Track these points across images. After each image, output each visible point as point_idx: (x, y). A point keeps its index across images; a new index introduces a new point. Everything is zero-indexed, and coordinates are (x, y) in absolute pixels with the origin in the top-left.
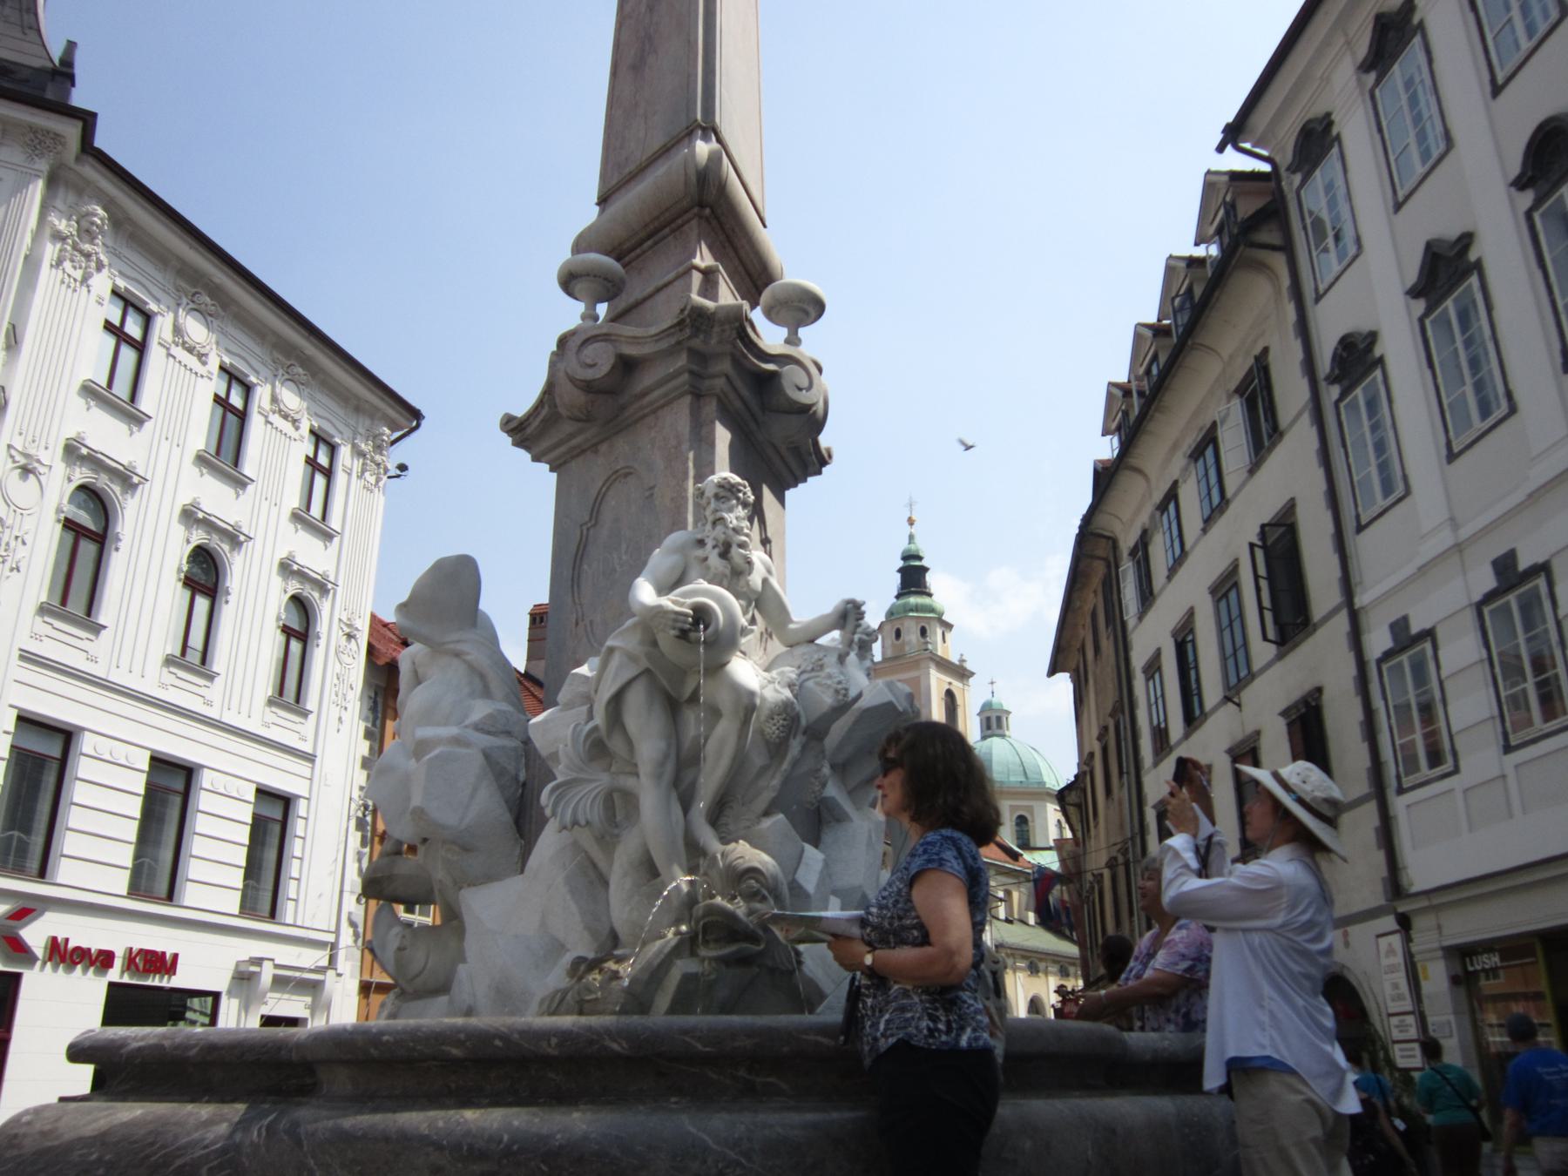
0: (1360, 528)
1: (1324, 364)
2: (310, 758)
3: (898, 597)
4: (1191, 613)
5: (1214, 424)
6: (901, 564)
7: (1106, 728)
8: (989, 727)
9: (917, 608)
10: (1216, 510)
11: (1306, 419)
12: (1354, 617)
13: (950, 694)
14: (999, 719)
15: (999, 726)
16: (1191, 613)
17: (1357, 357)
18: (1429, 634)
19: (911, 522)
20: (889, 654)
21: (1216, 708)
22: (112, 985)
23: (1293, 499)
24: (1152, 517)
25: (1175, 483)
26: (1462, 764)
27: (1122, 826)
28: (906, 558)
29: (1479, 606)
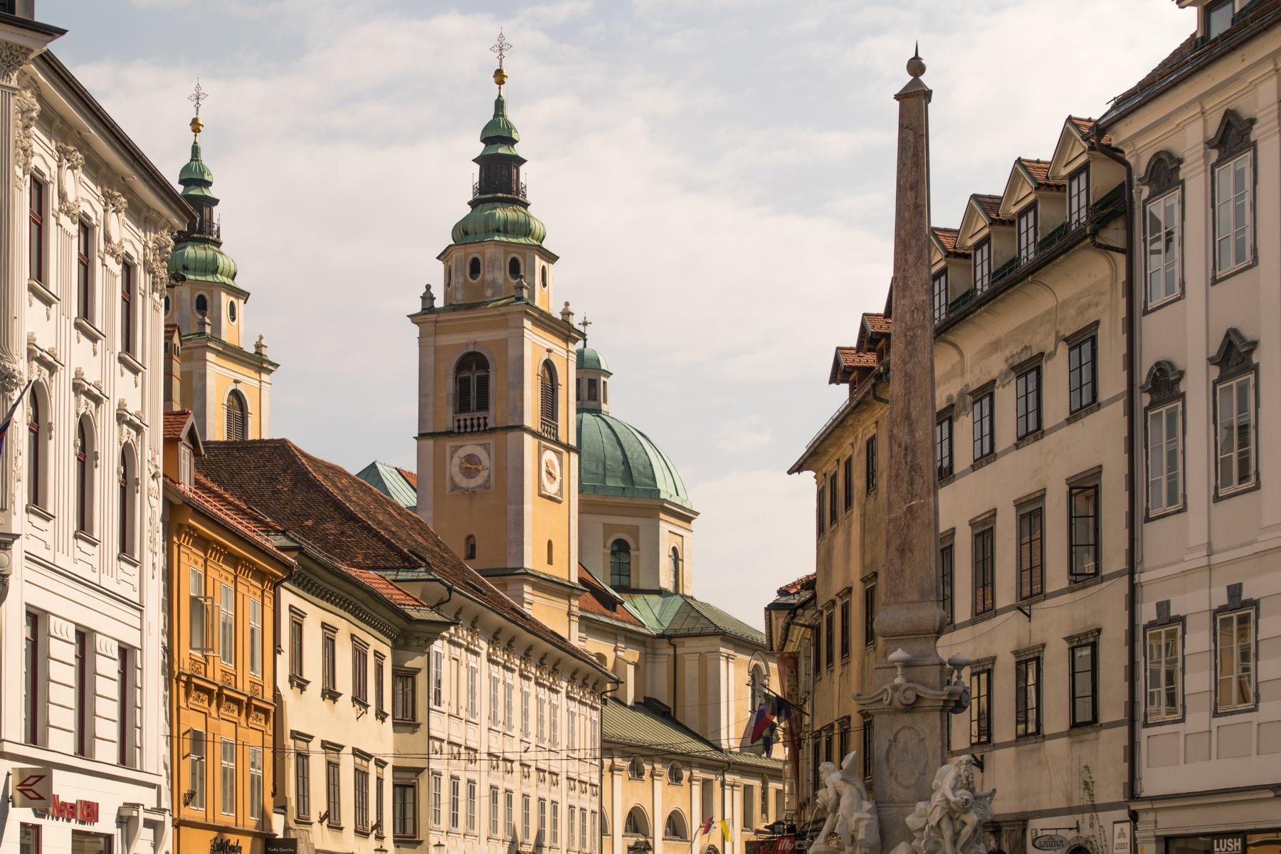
0: (1148, 519)
2: (139, 607)
3: (473, 204)
4: (993, 513)
6: (479, 148)
9: (507, 228)
11: (1119, 407)
12: (1133, 588)
13: (548, 365)
16: (993, 513)
18: (1182, 620)
20: (460, 297)
22: (75, 832)
23: (1100, 466)
24: (962, 395)
25: (994, 381)
26: (1187, 716)
29: (1216, 613)
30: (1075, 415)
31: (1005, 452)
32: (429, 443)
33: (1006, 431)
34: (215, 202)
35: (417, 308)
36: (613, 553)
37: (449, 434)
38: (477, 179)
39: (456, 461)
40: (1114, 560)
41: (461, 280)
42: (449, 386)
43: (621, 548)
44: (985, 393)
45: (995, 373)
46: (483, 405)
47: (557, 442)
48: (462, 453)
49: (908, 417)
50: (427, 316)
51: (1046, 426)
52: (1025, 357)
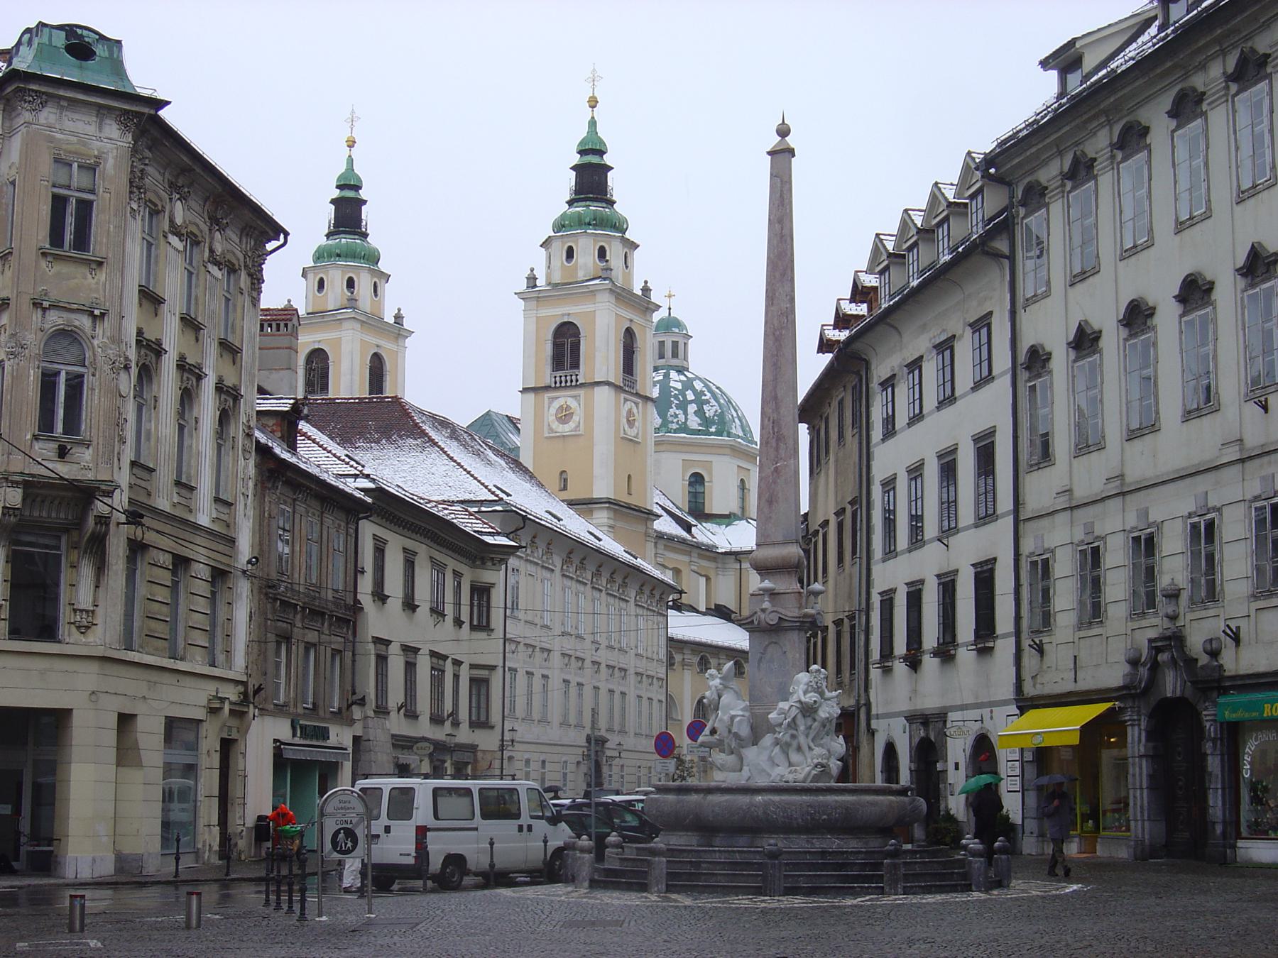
1: (1022, 357)
5: (954, 336)
7: (844, 510)
8: (662, 356)
10: (948, 399)
11: (1007, 379)
13: (629, 333)
14: (675, 344)
15: (675, 355)
17: (1037, 360)
19: (593, 103)
20: (557, 278)
21: (931, 541)
24: (900, 367)
27: (850, 597)
28: (582, 152)
30: (977, 386)
31: (931, 413)
32: (531, 396)
33: (931, 397)
34: (365, 202)
35: (523, 286)
36: (690, 484)
37: (547, 388)
38: (573, 183)
39: (553, 411)
40: (1005, 502)
41: (559, 264)
42: (548, 349)
43: (697, 479)
44: (915, 365)
45: (922, 351)
46: (575, 365)
47: (638, 395)
48: (556, 404)
49: (776, 398)
50: (532, 292)
51: (957, 394)
52: (943, 338)
